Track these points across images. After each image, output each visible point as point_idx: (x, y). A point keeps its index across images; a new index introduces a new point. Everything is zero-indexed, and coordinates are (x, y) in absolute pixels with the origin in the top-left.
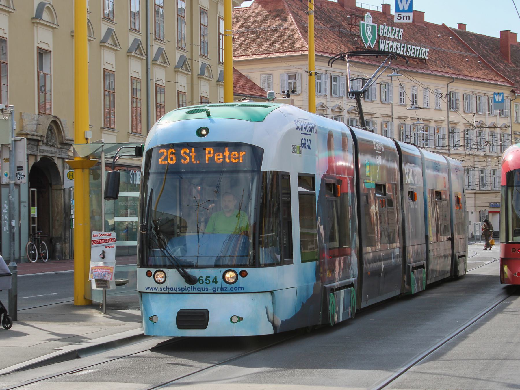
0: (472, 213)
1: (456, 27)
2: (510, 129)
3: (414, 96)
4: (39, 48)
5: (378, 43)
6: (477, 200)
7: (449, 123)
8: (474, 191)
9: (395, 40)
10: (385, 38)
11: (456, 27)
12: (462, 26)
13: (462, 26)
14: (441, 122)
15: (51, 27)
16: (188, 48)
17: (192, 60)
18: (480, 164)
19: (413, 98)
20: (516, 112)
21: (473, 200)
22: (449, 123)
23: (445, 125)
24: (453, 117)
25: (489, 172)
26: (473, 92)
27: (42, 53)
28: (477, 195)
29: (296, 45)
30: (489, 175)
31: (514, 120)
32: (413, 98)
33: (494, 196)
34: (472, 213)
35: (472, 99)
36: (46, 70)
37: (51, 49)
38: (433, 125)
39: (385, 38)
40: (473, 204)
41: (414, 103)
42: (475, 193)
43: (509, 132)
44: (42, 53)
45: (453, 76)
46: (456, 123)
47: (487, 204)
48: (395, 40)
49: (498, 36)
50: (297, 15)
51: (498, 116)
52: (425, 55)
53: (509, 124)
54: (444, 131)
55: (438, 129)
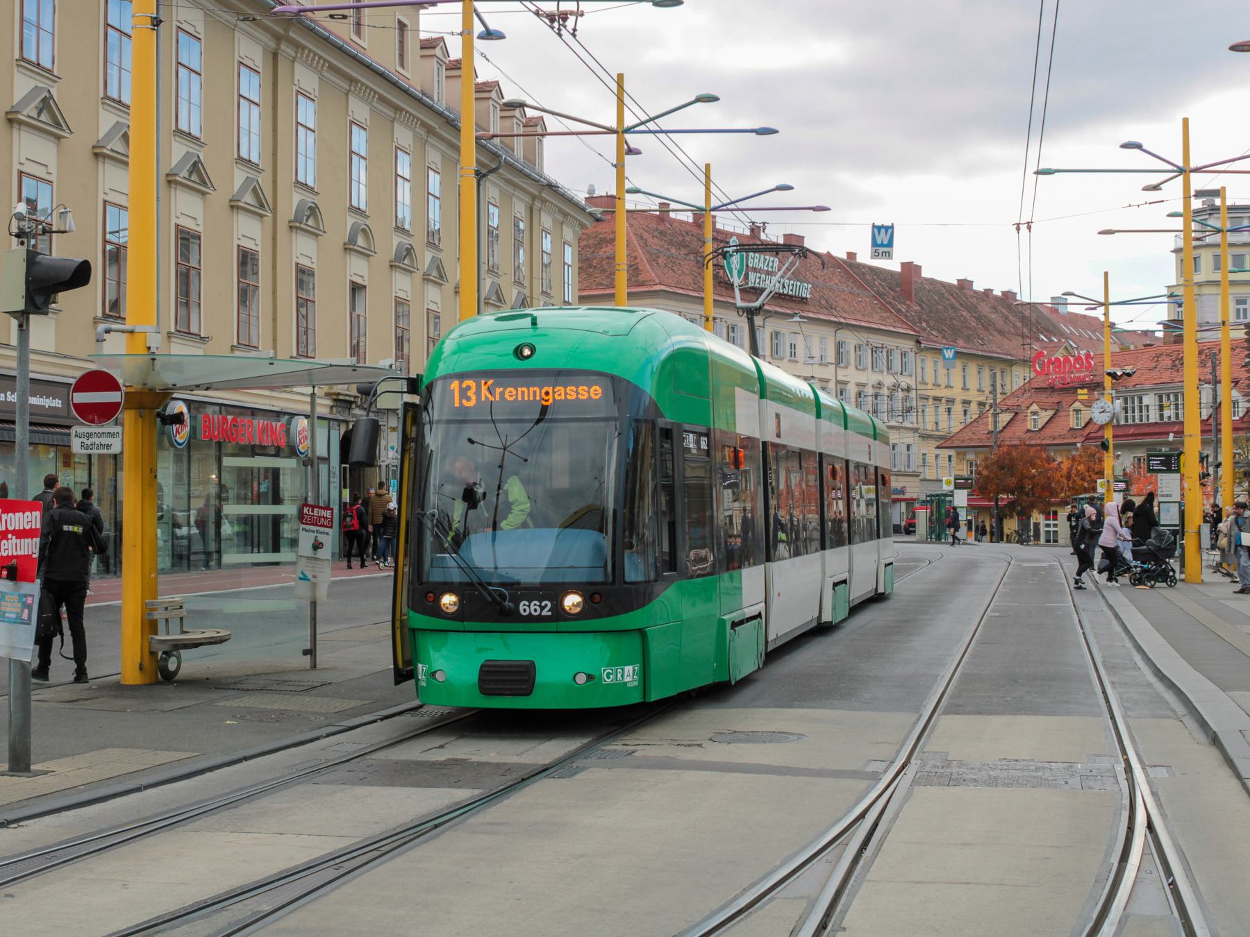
1: (845, 257)
3: (793, 346)
4: (353, 283)
5: (746, 277)
7: (838, 382)
9: (768, 273)
10: (755, 270)
11: (845, 257)
12: (851, 255)
13: (851, 255)
14: (827, 381)
15: (365, 254)
16: (526, 283)
17: (532, 298)
22: (838, 382)
27: (356, 288)
29: (641, 278)
31: (919, 379)
36: (359, 311)
37: (365, 283)
39: (755, 270)
41: (793, 354)
43: (913, 394)
44: (356, 288)
45: (842, 320)
46: (846, 383)
48: (768, 273)
49: (898, 269)
50: (642, 238)
52: (806, 294)
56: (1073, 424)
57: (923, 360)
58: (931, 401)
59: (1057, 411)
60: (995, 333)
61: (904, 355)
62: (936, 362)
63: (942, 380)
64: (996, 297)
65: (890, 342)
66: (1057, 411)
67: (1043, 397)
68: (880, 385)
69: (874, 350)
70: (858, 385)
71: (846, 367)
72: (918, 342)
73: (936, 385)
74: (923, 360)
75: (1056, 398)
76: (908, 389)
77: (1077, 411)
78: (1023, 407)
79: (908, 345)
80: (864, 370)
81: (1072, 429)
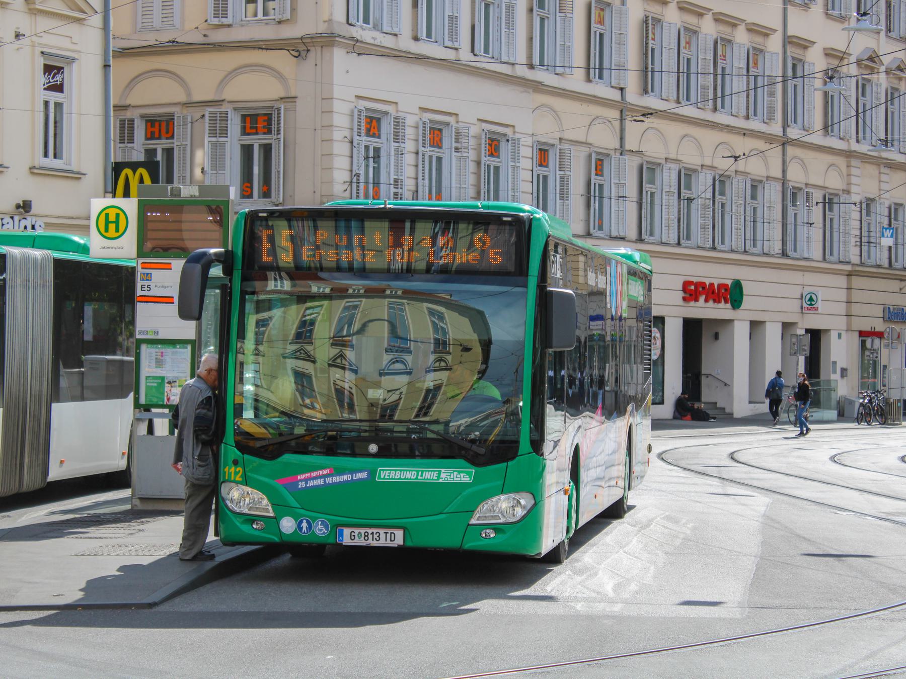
0: (840, 336)
6: (856, 296)
7: (788, 41)
8: (848, 268)
14: (764, 32)
21: (842, 295)
22: (788, 41)
23: (774, 44)
25: (886, 213)
28: (857, 282)
33: (895, 285)
34: (840, 336)
40: (842, 308)
42: (849, 275)
46: (804, 44)
47: (879, 311)
54: (773, 66)
55: (755, 55)
68: (871, 61)
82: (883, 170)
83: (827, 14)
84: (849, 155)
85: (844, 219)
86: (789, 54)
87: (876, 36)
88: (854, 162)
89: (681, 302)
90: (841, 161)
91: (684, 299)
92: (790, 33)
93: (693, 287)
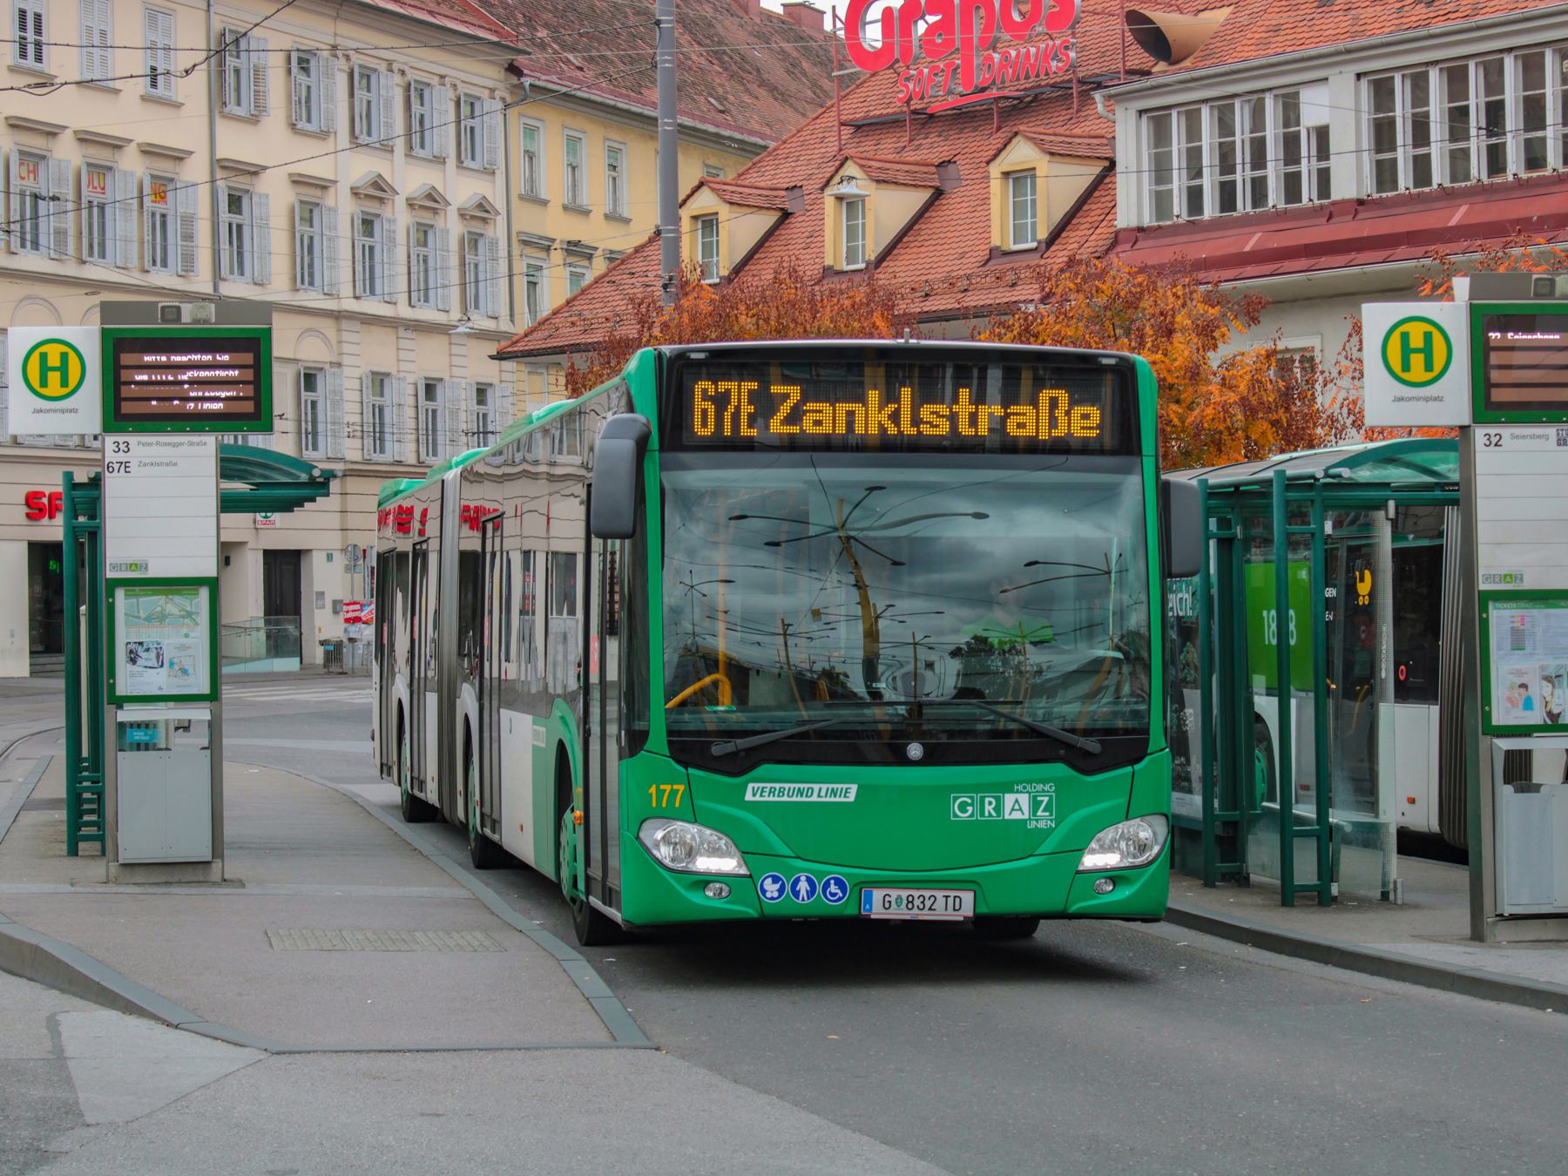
0: (330, 558)
2: (501, 222)
14: (178, 157)
18: (374, 351)
19: (23, 27)
20: (530, 156)
22: (222, 166)
23: (196, 170)
24: (236, 144)
25: (410, 390)
26: (334, 47)
30: (411, 401)
31: (519, 187)
32: (23, 27)
34: (330, 558)
35: (330, 75)
38: (132, 165)
43: (498, 230)
51: (451, 162)
53: (500, 205)
56: (1001, 234)
57: (531, 131)
58: (557, 256)
59: (938, 194)
60: (762, 92)
61: (466, 106)
62: (573, 143)
63: (595, 192)
64: (769, 16)
65: (425, 61)
66: (938, 194)
67: (887, 147)
69: (361, 78)
70: (298, 181)
71: (254, 120)
72: (514, 70)
73: (576, 209)
74: (531, 131)
75: (933, 148)
76: (481, 212)
77: (1020, 178)
78: (811, 186)
79: (482, 75)
80: (323, 135)
81: (995, 253)
82: (402, 333)
83: (293, 126)
84: (337, 316)
85: (333, 403)
86: (221, 184)
87: (388, 155)
88: (345, 324)
89: (24, 520)
90: (327, 326)
91: (28, 516)
92: (221, 154)
93: (45, 500)
